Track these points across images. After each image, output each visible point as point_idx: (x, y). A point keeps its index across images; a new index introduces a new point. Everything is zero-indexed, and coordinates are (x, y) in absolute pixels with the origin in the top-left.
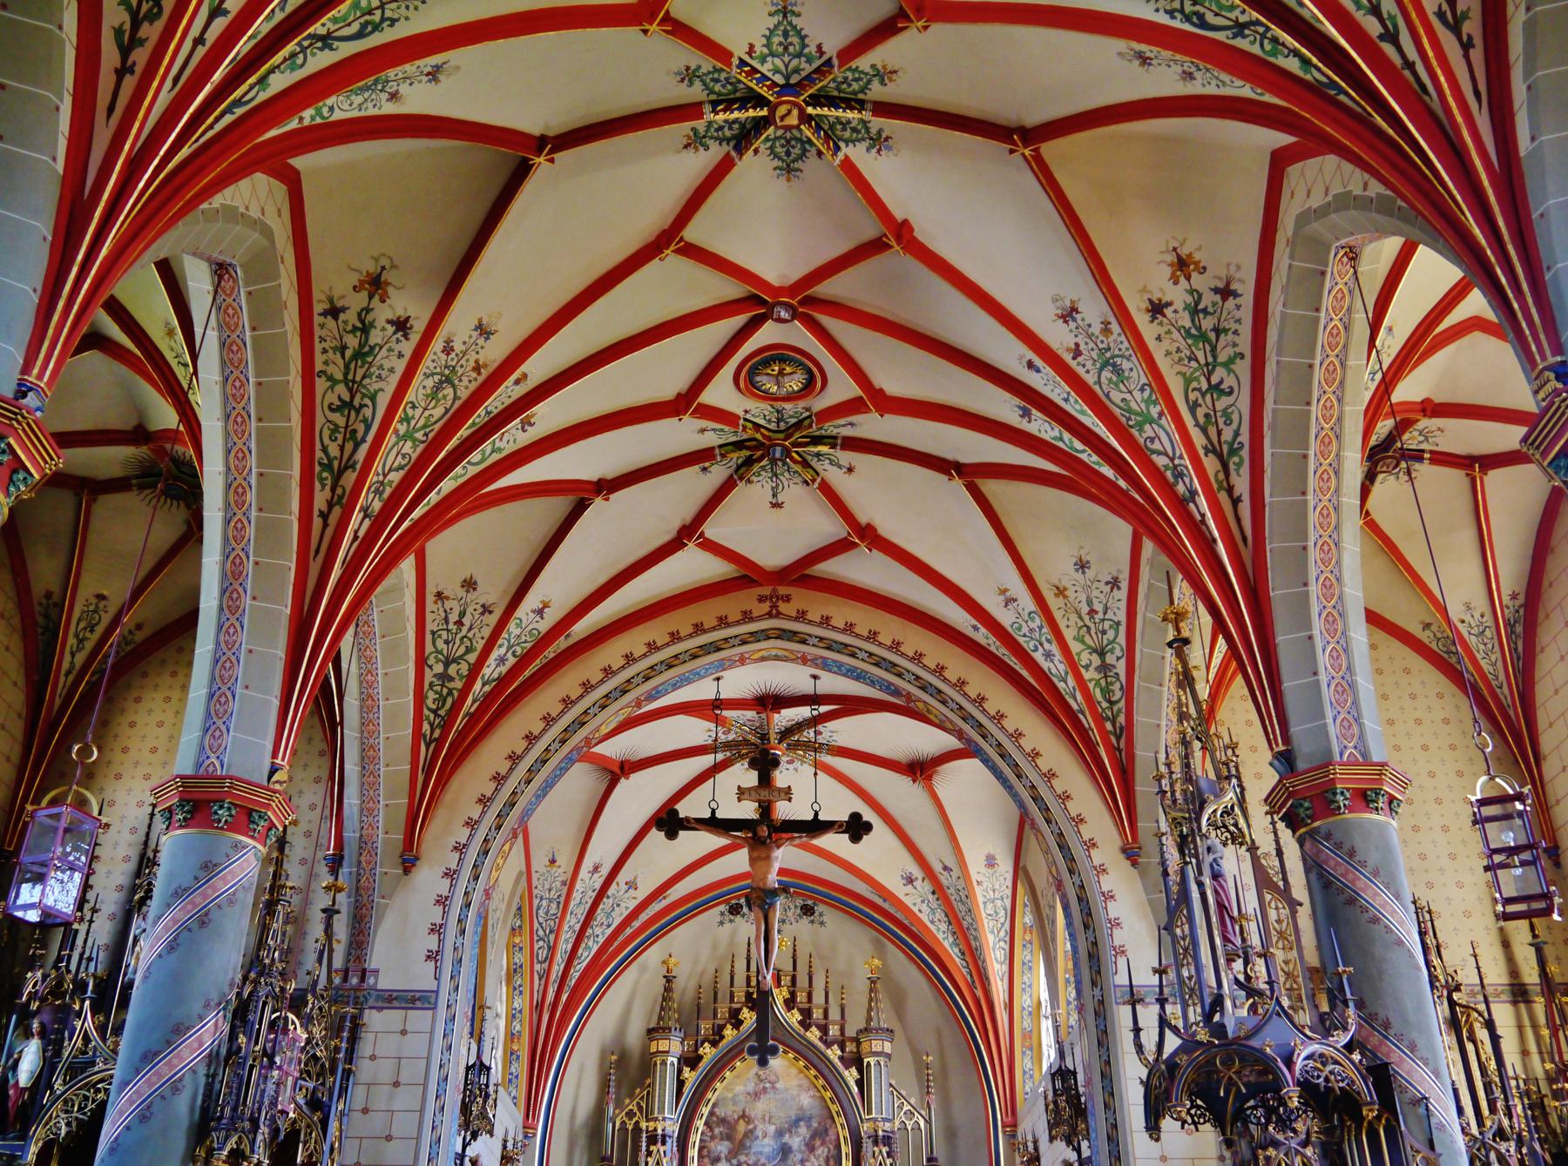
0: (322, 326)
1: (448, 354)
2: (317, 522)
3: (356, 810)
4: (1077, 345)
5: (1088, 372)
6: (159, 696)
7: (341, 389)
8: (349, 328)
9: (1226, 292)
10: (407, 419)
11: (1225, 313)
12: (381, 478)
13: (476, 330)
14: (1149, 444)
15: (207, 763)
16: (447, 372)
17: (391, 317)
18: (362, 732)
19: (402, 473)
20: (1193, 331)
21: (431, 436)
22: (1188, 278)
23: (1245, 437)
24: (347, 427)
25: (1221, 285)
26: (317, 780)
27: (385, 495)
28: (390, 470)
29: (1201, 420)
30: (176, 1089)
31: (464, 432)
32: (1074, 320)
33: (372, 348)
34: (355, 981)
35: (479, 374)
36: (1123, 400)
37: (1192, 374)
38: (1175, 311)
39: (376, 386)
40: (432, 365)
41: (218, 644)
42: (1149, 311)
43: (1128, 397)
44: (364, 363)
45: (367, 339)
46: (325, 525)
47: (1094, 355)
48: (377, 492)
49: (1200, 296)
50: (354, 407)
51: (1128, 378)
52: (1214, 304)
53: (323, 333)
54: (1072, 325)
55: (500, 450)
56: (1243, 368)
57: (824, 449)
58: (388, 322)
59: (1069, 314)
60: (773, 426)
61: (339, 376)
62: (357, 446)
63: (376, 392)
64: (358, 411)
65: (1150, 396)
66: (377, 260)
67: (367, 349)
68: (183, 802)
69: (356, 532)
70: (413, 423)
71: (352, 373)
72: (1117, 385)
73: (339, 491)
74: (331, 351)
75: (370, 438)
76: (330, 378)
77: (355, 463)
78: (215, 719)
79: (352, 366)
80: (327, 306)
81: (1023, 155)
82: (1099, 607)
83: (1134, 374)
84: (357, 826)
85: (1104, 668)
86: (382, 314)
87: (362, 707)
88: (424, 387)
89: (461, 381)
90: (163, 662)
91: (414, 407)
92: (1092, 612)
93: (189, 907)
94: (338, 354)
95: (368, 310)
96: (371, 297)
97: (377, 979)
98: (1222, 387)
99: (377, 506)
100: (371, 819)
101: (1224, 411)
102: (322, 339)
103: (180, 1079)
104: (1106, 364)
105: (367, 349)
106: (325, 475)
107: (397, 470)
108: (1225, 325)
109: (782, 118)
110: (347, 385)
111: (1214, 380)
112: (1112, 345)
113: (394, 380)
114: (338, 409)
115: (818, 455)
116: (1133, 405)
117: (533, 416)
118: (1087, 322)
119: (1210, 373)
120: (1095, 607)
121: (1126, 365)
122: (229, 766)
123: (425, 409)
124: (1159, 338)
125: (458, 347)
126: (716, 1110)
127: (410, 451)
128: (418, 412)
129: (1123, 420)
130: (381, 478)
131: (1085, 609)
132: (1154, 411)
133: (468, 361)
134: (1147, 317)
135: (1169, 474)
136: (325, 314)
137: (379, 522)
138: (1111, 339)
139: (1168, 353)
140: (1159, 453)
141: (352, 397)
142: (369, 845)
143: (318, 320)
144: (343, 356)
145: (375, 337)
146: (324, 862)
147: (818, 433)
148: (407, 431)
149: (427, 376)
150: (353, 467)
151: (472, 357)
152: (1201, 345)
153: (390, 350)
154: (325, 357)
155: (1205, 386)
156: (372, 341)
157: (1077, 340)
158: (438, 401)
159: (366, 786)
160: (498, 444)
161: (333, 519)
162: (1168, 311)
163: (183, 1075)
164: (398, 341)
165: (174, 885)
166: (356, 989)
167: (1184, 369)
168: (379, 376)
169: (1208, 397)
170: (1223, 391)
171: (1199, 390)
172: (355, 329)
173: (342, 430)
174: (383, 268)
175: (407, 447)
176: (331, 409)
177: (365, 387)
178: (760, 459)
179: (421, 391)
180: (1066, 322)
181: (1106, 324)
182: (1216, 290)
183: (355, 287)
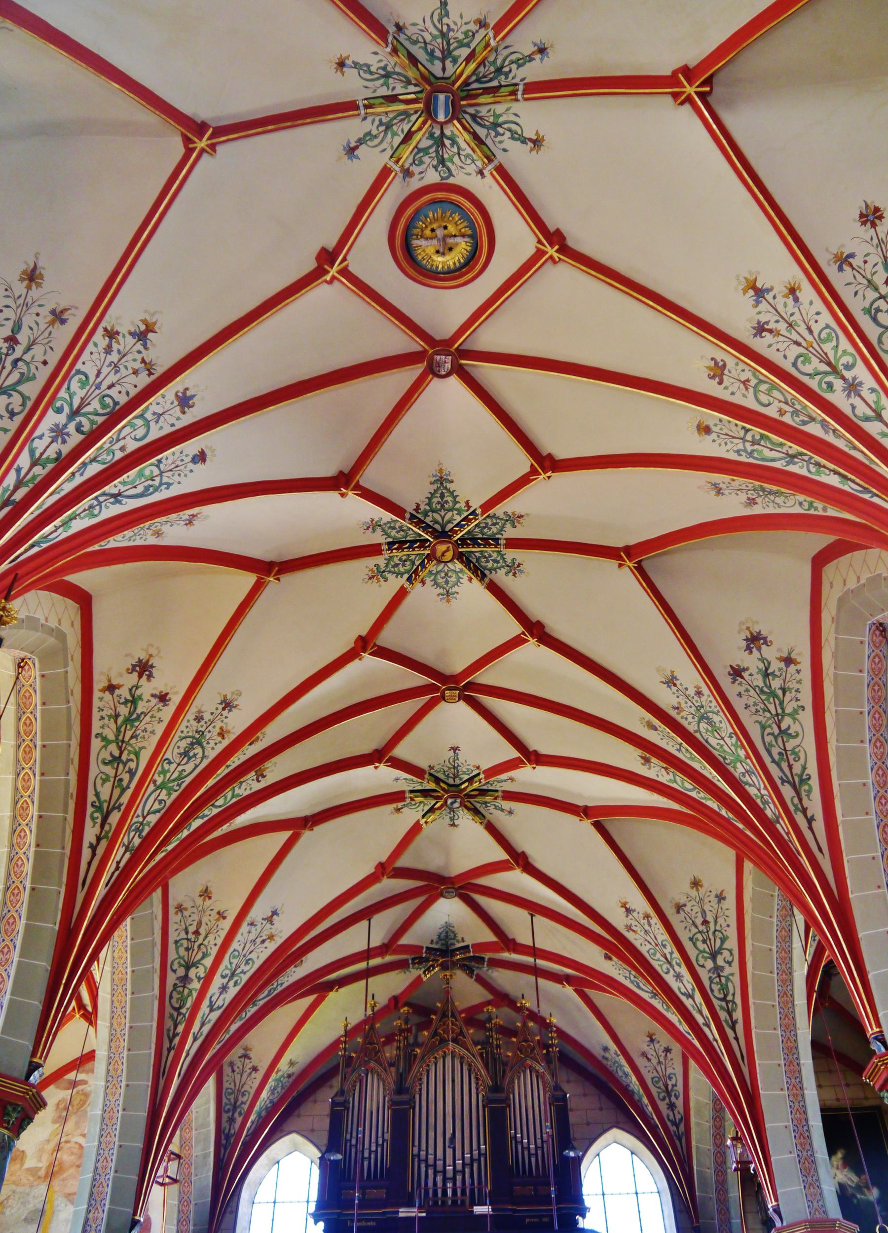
0: (101, 699)
1: (199, 722)
2: (86, 853)
4: (679, 703)
5: (690, 723)
7: (114, 749)
8: (122, 700)
9: (788, 661)
10: (164, 772)
11: (788, 676)
12: (141, 819)
13: (221, 703)
14: (742, 778)
16: (197, 736)
17: (154, 692)
19: (158, 815)
20: (765, 689)
21: (184, 785)
22: (759, 650)
23: (813, 769)
24: (116, 776)
25: (785, 655)
27: (144, 834)
28: (148, 814)
29: (776, 757)
31: (210, 783)
32: (675, 685)
33: (139, 716)
35: (223, 738)
36: (718, 744)
37: (767, 721)
38: (751, 675)
39: (140, 745)
40: (185, 730)
42: (730, 674)
43: (722, 742)
44: (132, 726)
45: (135, 709)
46: (94, 854)
47: (693, 710)
48: (137, 830)
49: (769, 663)
50: (122, 761)
51: (720, 728)
52: (780, 669)
53: (101, 704)
54: (674, 689)
55: (238, 795)
56: (807, 718)
57: (488, 799)
58: (153, 696)
59: (671, 681)
60: (451, 781)
61: (111, 737)
62: (123, 791)
63: (141, 748)
64: (125, 764)
65: (736, 743)
66: (147, 651)
67: (134, 716)
69: (118, 863)
70: (168, 775)
71: (122, 734)
72: (712, 732)
73: (107, 828)
74: (107, 718)
75: (133, 786)
76: (104, 739)
77: (120, 805)
79: (123, 729)
80: (106, 684)
81: (629, 566)
82: (710, 918)
83: (723, 725)
85: (717, 969)
86: (147, 688)
88: (179, 747)
89: (208, 743)
91: (170, 763)
92: (705, 922)
94: (112, 720)
95: (137, 687)
96: (140, 676)
98: (789, 732)
99: (137, 841)
101: (793, 750)
102: (101, 710)
104: (702, 718)
105: (134, 716)
106: (96, 815)
107: (155, 812)
108: (790, 685)
109: (448, 550)
110: (118, 744)
111: (784, 726)
112: (704, 703)
113: (155, 739)
114: (110, 763)
115: (486, 803)
116: (726, 747)
117: (264, 770)
118: (684, 686)
119: (780, 721)
120: (708, 919)
121: (716, 719)
123: (179, 764)
124: (740, 695)
125: (207, 717)
127: (165, 798)
128: (174, 766)
129: (721, 759)
130: (141, 819)
131: (699, 921)
132: (742, 753)
133: (214, 727)
134: (729, 679)
135: (758, 801)
136: (103, 690)
137: (137, 856)
138: (703, 699)
139: (747, 707)
140: (750, 785)
141: (121, 753)
143: (97, 694)
144: (116, 722)
145: (141, 707)
147: (485, 787)
148: (163, 782)
149: (182, 739)
150: (119, 808)
151: (218, 724)
152: (771, 700)
153: (152, 717)
154: (101, 723)
155: (776, 731)
156: (139, 711)
157: (678, 700)
158: (190, 758)
160: (237, 791)
161: (100, 851)
162: (745, 675)
164: (159, 710)
167: (760, 719)
168: (144, 738)
169: (780, 740)
170: (790, 735)
171: (773, 734)
172: (127, 701)
173: (112, 779)
174: (151, 656)
175: (163, 795)
176: (105, 763)
177: (131, 745)
178: (439, 808)
179: (176, 751)
180: (669, 686)
181: (698, 687)
182: (781, 659)
183: (128, 669)
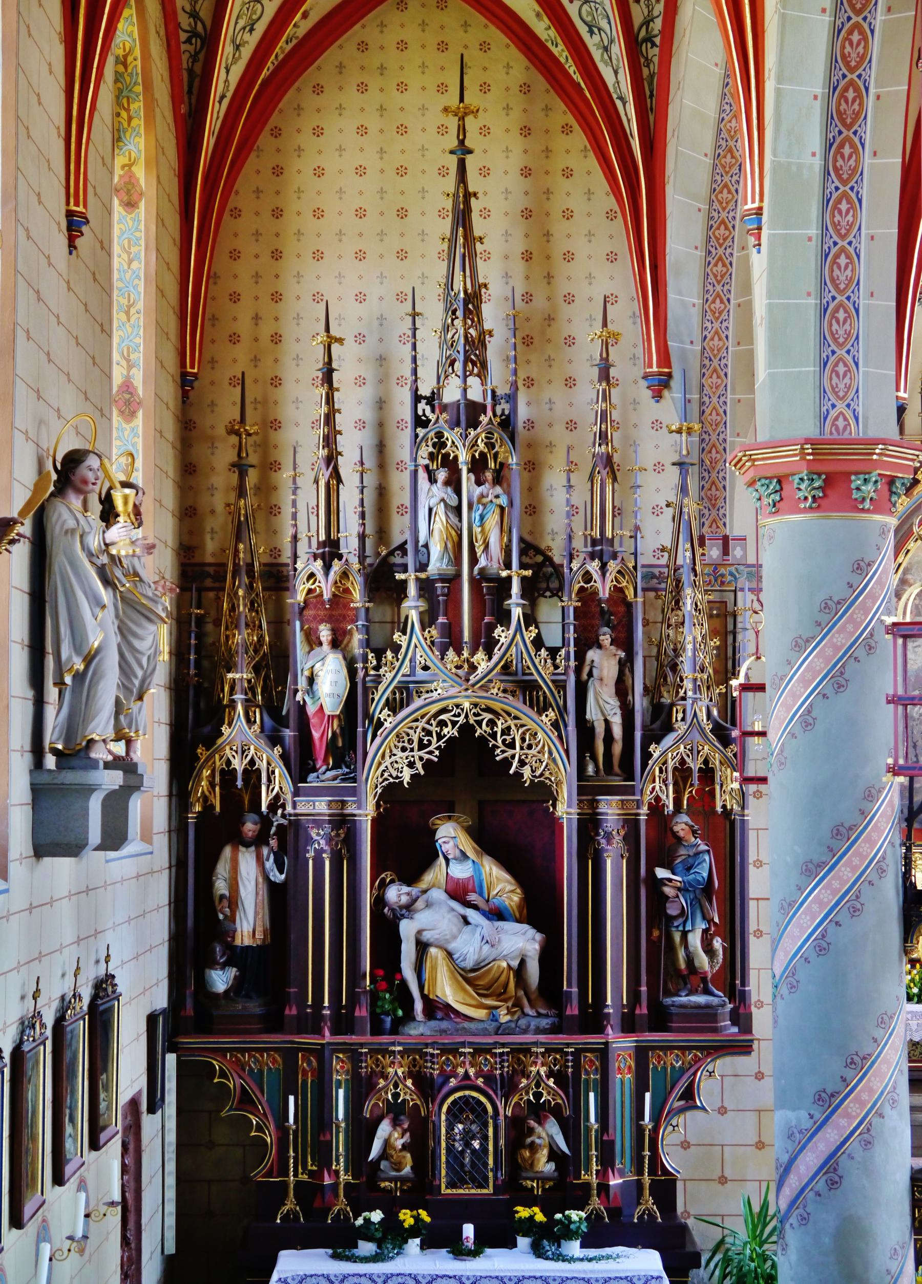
3: (695, 314)
6: (349, 124)
15: (833, 413)
18: (711, 202)
26: (612, 258)
30: (881, 871)
34: (714, 553)
41: (824, 228)
68: (813, 474)
78: (833, 347)
84: (698, 339)
87: (715, 166)
90: (341, 67)
93: (850, 627)
97: (745, 549)
100: (717, 325)
103: (883, 858)
122: (866, 418)
126: (909, 577)
142: (715, 362)
146: (644, 384)
159: (712, 279)
163: (885, 852)
165: (821, 596)
166: (716, 567)
